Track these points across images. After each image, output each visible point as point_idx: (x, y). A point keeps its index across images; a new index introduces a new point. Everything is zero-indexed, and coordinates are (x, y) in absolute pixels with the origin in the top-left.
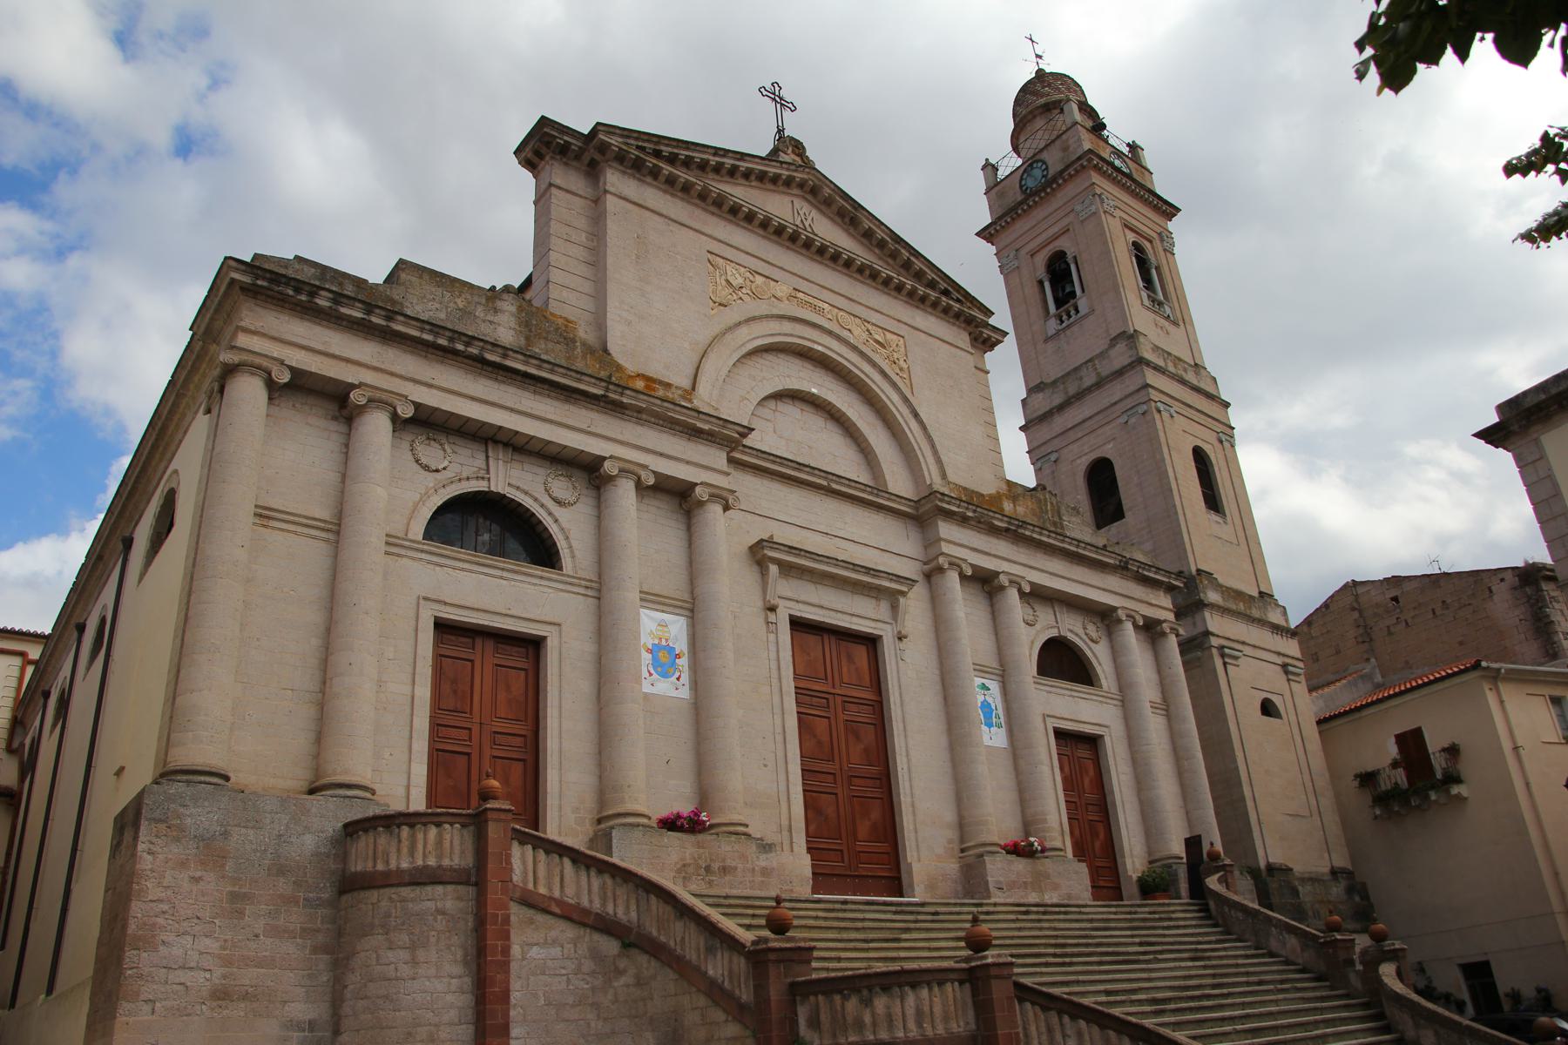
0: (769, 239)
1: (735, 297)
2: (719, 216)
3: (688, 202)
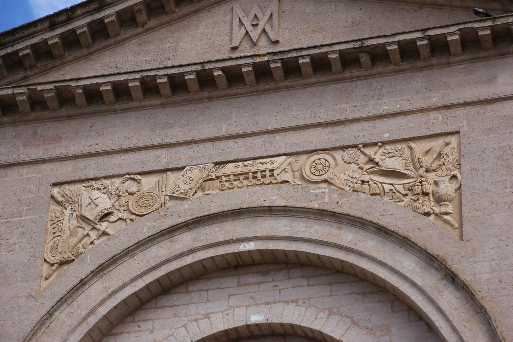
0: (173, 104)
1: (94, 235)
2: (81, 115)
3: (25, 122)
